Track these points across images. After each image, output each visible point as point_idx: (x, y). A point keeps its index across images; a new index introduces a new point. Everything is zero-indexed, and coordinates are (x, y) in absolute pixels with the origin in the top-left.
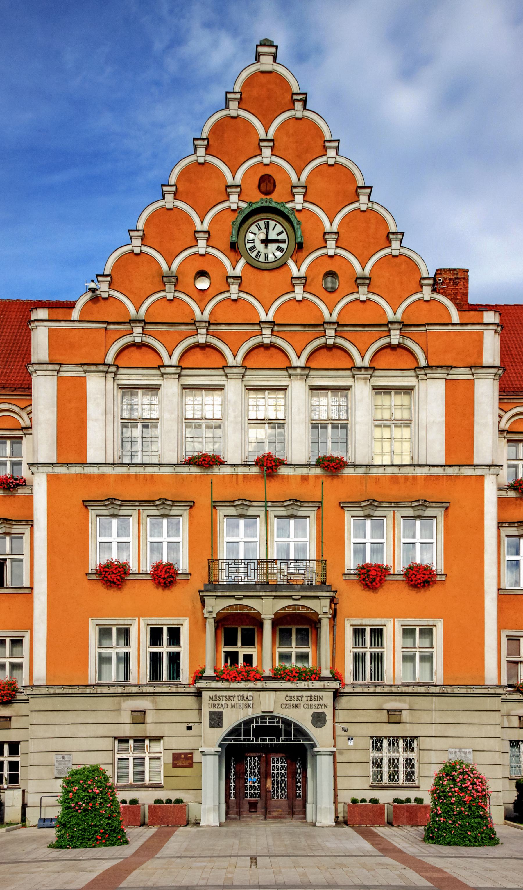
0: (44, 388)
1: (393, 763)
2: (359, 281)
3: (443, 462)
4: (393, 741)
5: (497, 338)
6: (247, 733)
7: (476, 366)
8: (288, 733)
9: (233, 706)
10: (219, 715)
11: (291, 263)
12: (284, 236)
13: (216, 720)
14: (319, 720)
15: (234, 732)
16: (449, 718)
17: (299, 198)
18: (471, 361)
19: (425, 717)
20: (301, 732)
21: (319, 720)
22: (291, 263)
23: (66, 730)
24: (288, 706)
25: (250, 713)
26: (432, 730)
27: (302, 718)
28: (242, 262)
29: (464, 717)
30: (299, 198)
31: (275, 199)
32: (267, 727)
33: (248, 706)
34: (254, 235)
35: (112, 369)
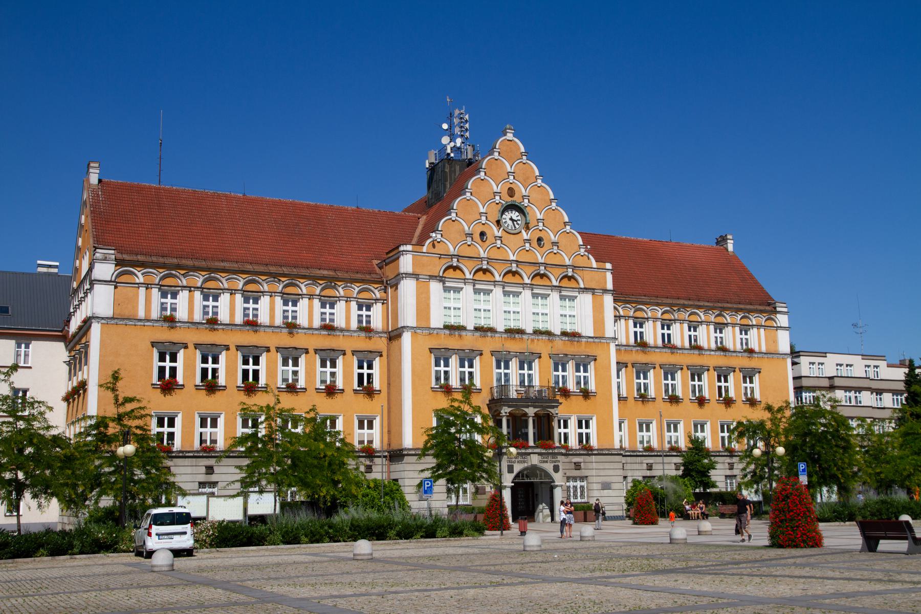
0: (408, 288)
1: (575, 487)
2: (554, 244)
6: (523, 476)
7: (605, 291)
8: (541, 476)
10: (512, 466)
11: (523, 231)
12: (519, 218)
13: (510, 469)
14: (556, 469)
15: (517, 476)
16: (601, 466)
17: (526, 201)
20: (547, 475)
21: (556, 469)
22: (523, 231)
25: (526, 465)
26: (594, 473)
27: (549, 467)
29: (607, 466)
30: (526, 201)
31: (517, 199)
33: (524, 462)
34: (508, 216)
35: (442, 279)
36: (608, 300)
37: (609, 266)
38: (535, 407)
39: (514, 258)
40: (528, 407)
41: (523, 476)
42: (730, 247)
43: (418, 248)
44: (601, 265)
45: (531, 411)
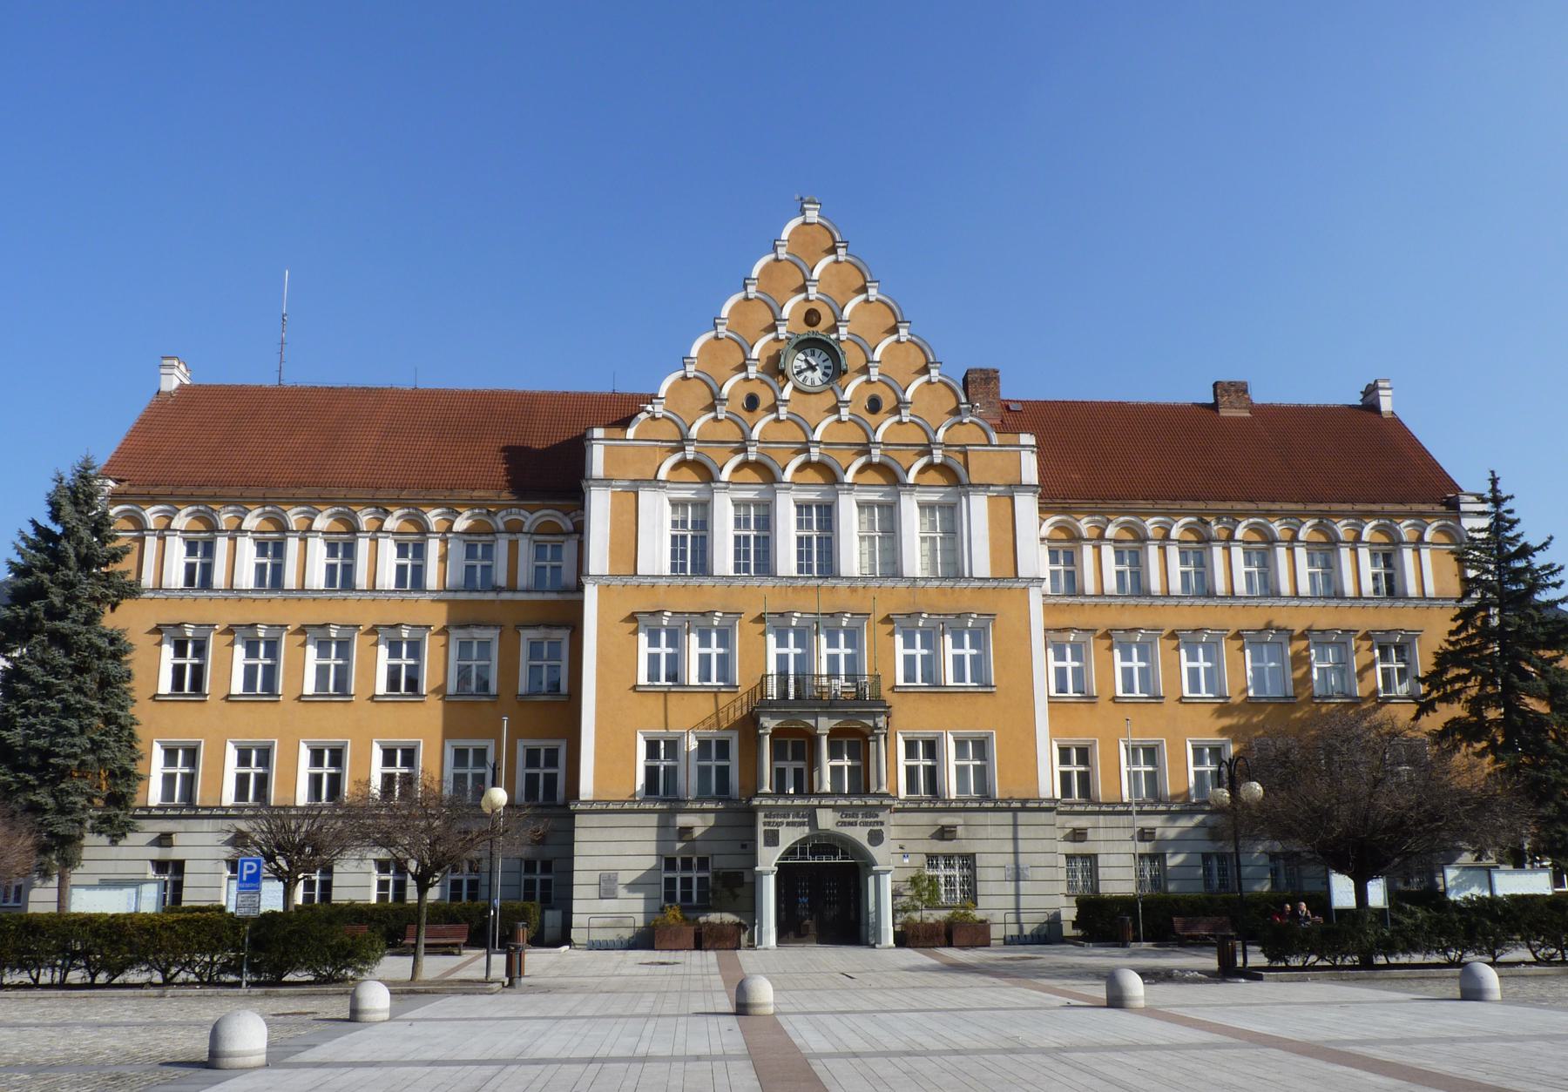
0: (600, 504)
3: (988, 575)
4: (948, 857)
5: (1034, 457)
6: (803, 852)
7: (1019, 486)
9: (788, 824)
13: (772, 839)
15: (791, 852)
18: (1011, 479)
19: (981, 832)
21: (876, 838)
23: (613, 848)
24: (844, 824)
27: (859, 834)
28: (789, 388)
32: (825, 844)
36: (1027, 505)
37: (1027, 439)
38: (831, 716)
39: (817, 436)
40: (815, 716)
41: (803, 852)
42: (1386, 404)
43: (616, 432)
44: (1009, 438)
45: (825, 725)
